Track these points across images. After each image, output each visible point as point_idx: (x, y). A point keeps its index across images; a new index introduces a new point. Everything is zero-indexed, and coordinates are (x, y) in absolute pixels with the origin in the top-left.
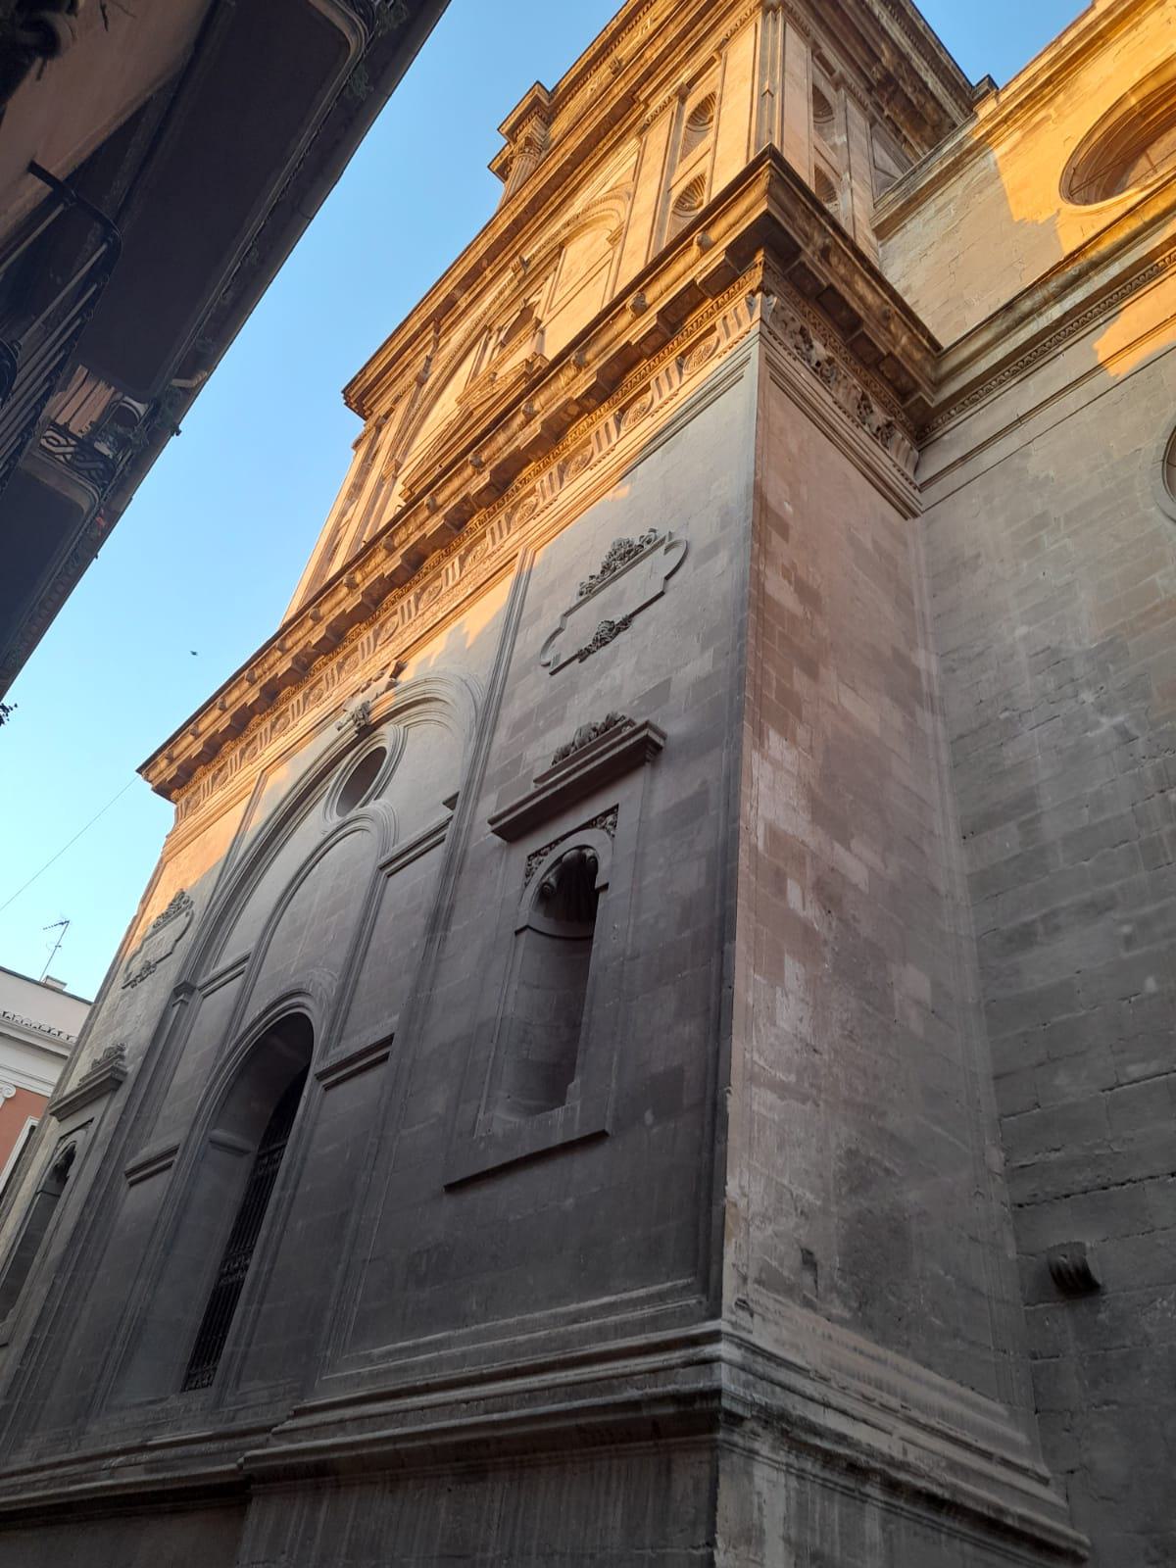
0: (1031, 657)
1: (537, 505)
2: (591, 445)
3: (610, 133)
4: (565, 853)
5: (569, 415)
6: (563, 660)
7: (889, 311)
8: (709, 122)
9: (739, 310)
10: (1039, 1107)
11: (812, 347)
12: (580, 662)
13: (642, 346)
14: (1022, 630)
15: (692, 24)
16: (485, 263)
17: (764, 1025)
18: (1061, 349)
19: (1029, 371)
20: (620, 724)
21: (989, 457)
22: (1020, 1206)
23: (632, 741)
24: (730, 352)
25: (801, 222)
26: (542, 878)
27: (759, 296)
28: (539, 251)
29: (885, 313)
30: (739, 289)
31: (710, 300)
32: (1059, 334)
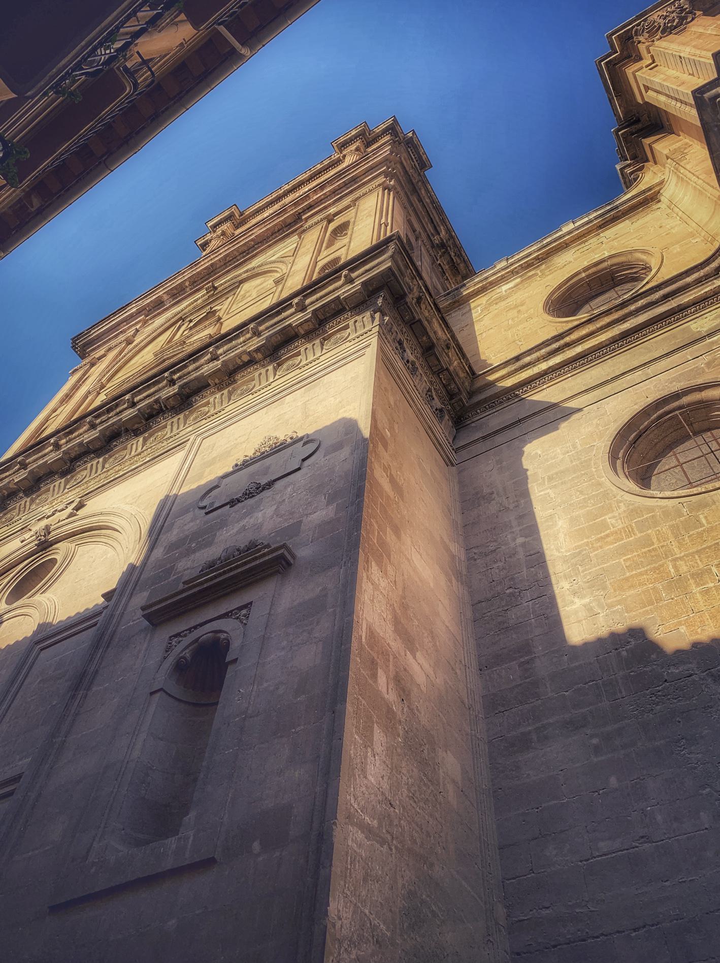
0: (526, 556)
1: (208, 411)
2: (254, 382)
4: (201, 636)
6: (216, 505)
8: (344, 236)
10: (533, 873)
11: (405, 351)
12: (230, 507)
13: (299, 328)
14: (520, 540)
15: (340, 187)
16: (187, 284)
17: (359, 775)
18: (545, 387)
20: (260, 546)
22: (518, 954)
24: (357, 340)
26: (180, 653)
28: (225, 283)
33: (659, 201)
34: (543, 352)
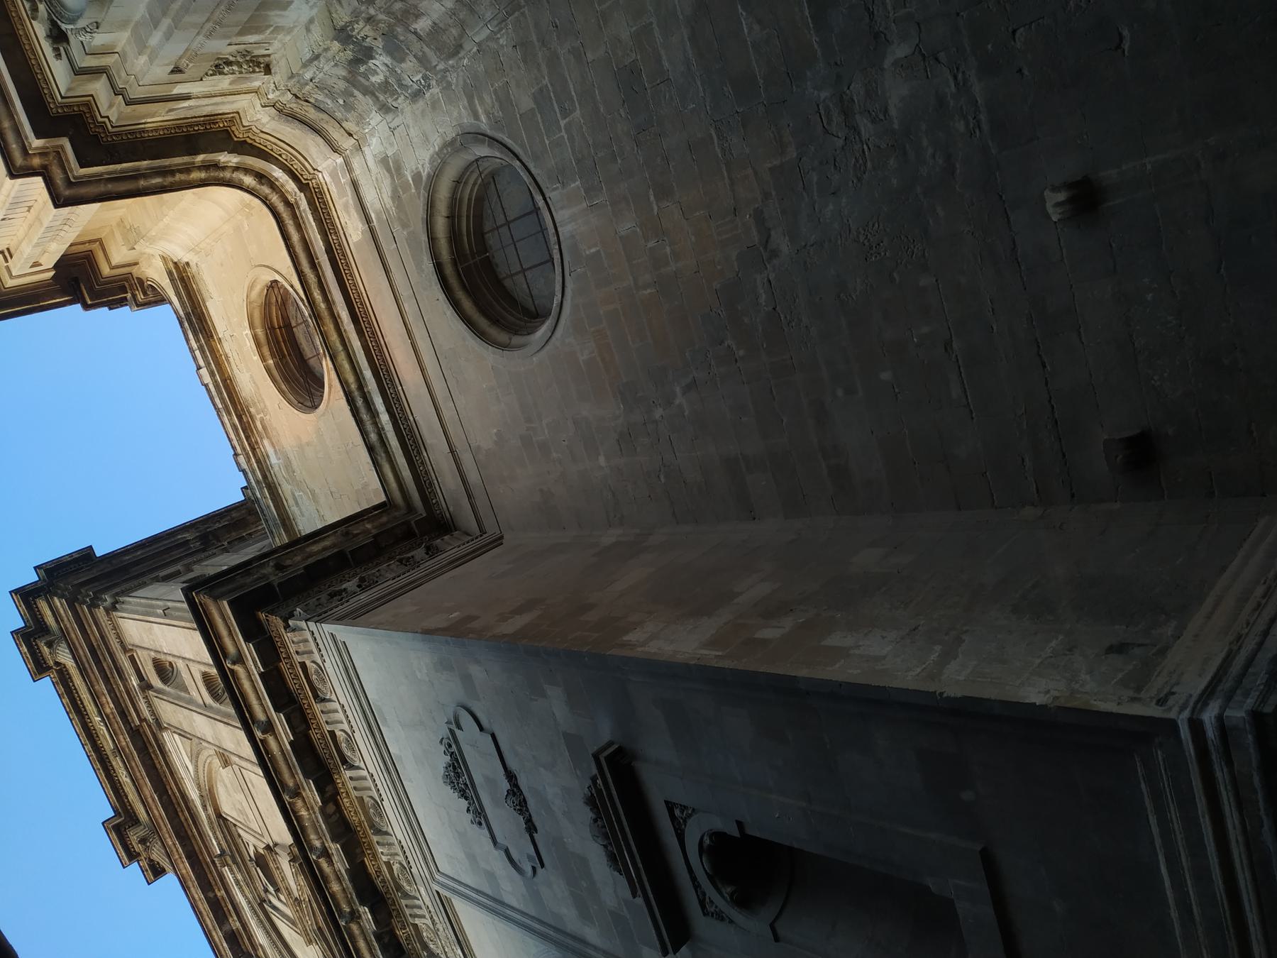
1: (400, 864)
2: (364, 797)
3: (153, 756)
4: (706, 871)
5: (334, 813)
6: (532, 851)
7: (342, 531)
8: (173, 668)
9: (295, 639)
12: (537, 833)
14: (602, 460)
16: (211, 895)
17: (883, 665)
18: (411, 418)
19: (420, 441)
20: (594, 791)
21: (473, 477)
23: (608, 776)
24: (324, 652)
25: (249, 580)
26: (726, 901)
27: (291, 622)
28: (217, 838)
29: (342, 535)
30: (280, 637)
31: (281, 664)
32: (400, 418)
33: (188, 264)
34: (365, 417)
